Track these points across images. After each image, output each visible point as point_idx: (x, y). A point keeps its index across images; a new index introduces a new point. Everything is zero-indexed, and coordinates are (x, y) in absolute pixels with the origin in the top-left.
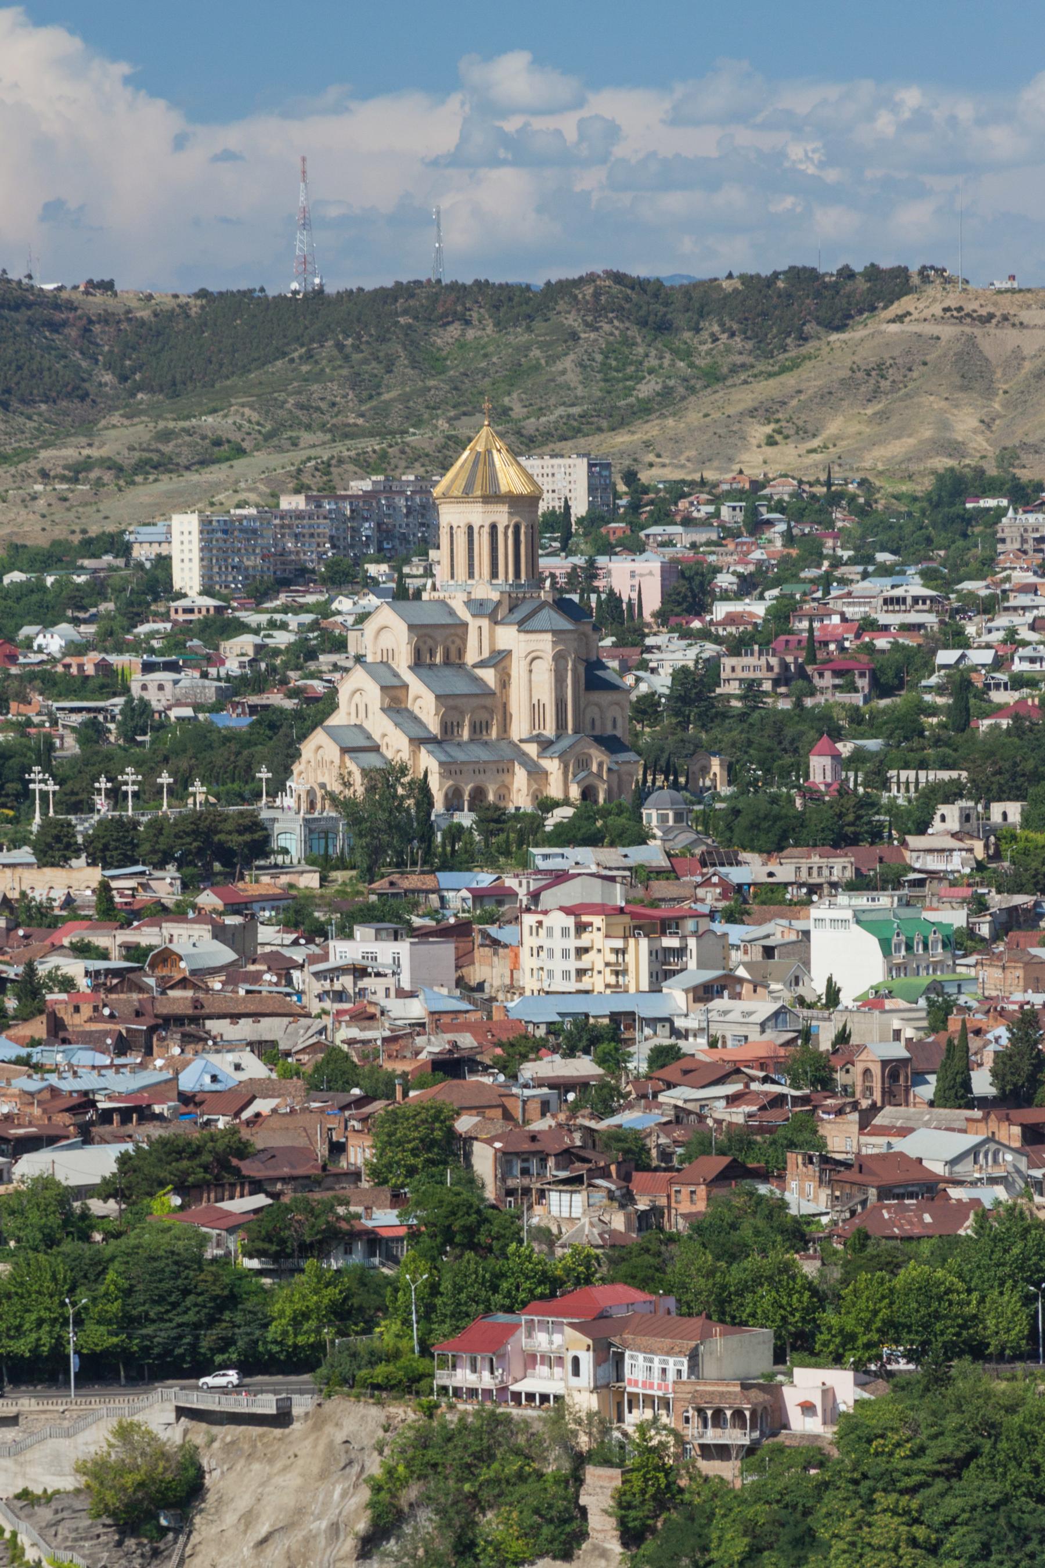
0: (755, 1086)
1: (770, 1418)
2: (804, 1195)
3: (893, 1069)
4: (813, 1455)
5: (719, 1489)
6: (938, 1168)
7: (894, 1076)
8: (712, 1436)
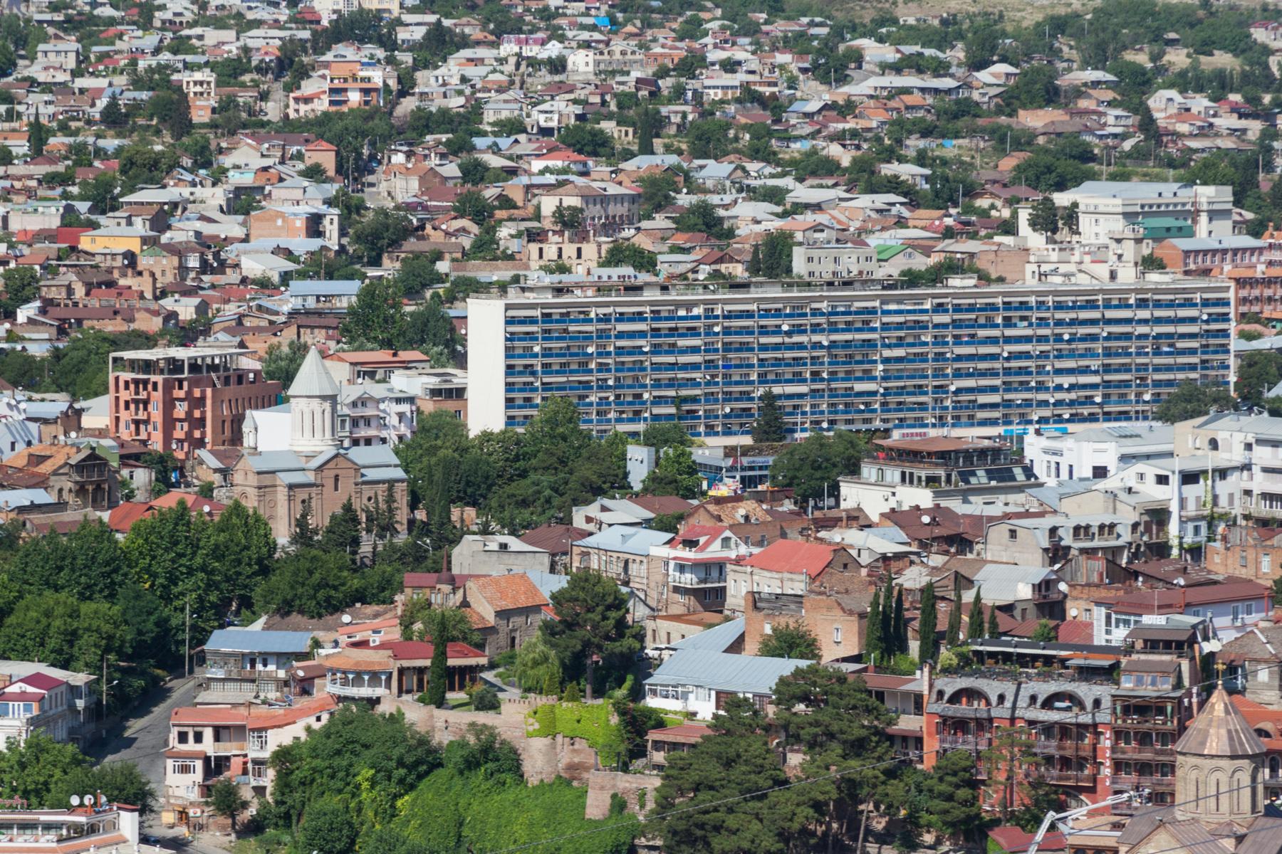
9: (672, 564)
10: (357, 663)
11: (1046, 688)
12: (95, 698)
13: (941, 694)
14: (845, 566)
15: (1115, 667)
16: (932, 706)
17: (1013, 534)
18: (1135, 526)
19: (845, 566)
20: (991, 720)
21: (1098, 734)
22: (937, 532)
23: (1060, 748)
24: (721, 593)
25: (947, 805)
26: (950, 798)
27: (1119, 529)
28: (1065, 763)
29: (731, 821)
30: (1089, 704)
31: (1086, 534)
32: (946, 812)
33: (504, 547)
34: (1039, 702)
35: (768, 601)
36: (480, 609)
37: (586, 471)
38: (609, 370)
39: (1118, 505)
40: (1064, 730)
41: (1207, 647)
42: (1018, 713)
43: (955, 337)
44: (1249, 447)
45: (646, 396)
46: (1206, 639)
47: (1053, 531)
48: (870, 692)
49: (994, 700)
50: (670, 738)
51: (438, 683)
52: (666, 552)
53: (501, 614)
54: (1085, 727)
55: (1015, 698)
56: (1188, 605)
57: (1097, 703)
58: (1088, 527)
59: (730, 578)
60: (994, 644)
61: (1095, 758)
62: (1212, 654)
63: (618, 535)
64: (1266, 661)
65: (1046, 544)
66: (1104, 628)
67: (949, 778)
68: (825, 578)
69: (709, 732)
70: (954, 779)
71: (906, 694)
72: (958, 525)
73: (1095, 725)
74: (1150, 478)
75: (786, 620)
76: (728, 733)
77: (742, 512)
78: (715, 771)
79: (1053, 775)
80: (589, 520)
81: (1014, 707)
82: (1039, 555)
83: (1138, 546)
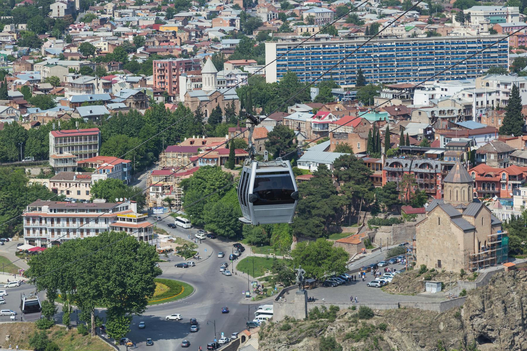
9: (313, 124)
11: (421, 162)
12: (131, 168)
13: (387, 164)
14: (365, 124)
15: (442, 154)
16: (385, 168)
17: (420, 113)
18: (460, 111)
19: (365, 124)
20: (403, 172)
22: (399, 113)
23: (425, 181)
25: (387, 200)
26: (388, 197)
27: (454, 111)
28: (426, 185)
29: (318, 205)
30: (434, 167)
31: (444, 113)
32: (387, 202)
35: (337, 135)
37: (295, 95)
38: (309, 65)
39: (456, 104)
41: (472, 148)
43: (397, 49)
44: (498, 85)
45: (321, 73)
46: (473, 145)
47: (432, 112)
48: (365, 164)
49: (404, 165)
50: (303, 179)
52: (312, 120)
54: (433, 174)
55: (409, 164)
56: (469, 135)
57: (437, 166)
58: (444, 111)
60: (411, 148)
61: (436, 184)
62: (475, 151)
64: (493, 153)
65: (430, 116)
66: (443, 142)
67: (388, 191)
68: (358, 128)
69: (312, 177)
70: (390, 191)
71: (377, 164)
72: (407, 111)
73: (436, 173)
74: (466, 96)
75: (343, 142)
76: (318, 177)
77: (337, 107)
78: (313, 188)
79: (422, 190)
80: (292, 110)
81: (410, 168)
83: (461, 117)
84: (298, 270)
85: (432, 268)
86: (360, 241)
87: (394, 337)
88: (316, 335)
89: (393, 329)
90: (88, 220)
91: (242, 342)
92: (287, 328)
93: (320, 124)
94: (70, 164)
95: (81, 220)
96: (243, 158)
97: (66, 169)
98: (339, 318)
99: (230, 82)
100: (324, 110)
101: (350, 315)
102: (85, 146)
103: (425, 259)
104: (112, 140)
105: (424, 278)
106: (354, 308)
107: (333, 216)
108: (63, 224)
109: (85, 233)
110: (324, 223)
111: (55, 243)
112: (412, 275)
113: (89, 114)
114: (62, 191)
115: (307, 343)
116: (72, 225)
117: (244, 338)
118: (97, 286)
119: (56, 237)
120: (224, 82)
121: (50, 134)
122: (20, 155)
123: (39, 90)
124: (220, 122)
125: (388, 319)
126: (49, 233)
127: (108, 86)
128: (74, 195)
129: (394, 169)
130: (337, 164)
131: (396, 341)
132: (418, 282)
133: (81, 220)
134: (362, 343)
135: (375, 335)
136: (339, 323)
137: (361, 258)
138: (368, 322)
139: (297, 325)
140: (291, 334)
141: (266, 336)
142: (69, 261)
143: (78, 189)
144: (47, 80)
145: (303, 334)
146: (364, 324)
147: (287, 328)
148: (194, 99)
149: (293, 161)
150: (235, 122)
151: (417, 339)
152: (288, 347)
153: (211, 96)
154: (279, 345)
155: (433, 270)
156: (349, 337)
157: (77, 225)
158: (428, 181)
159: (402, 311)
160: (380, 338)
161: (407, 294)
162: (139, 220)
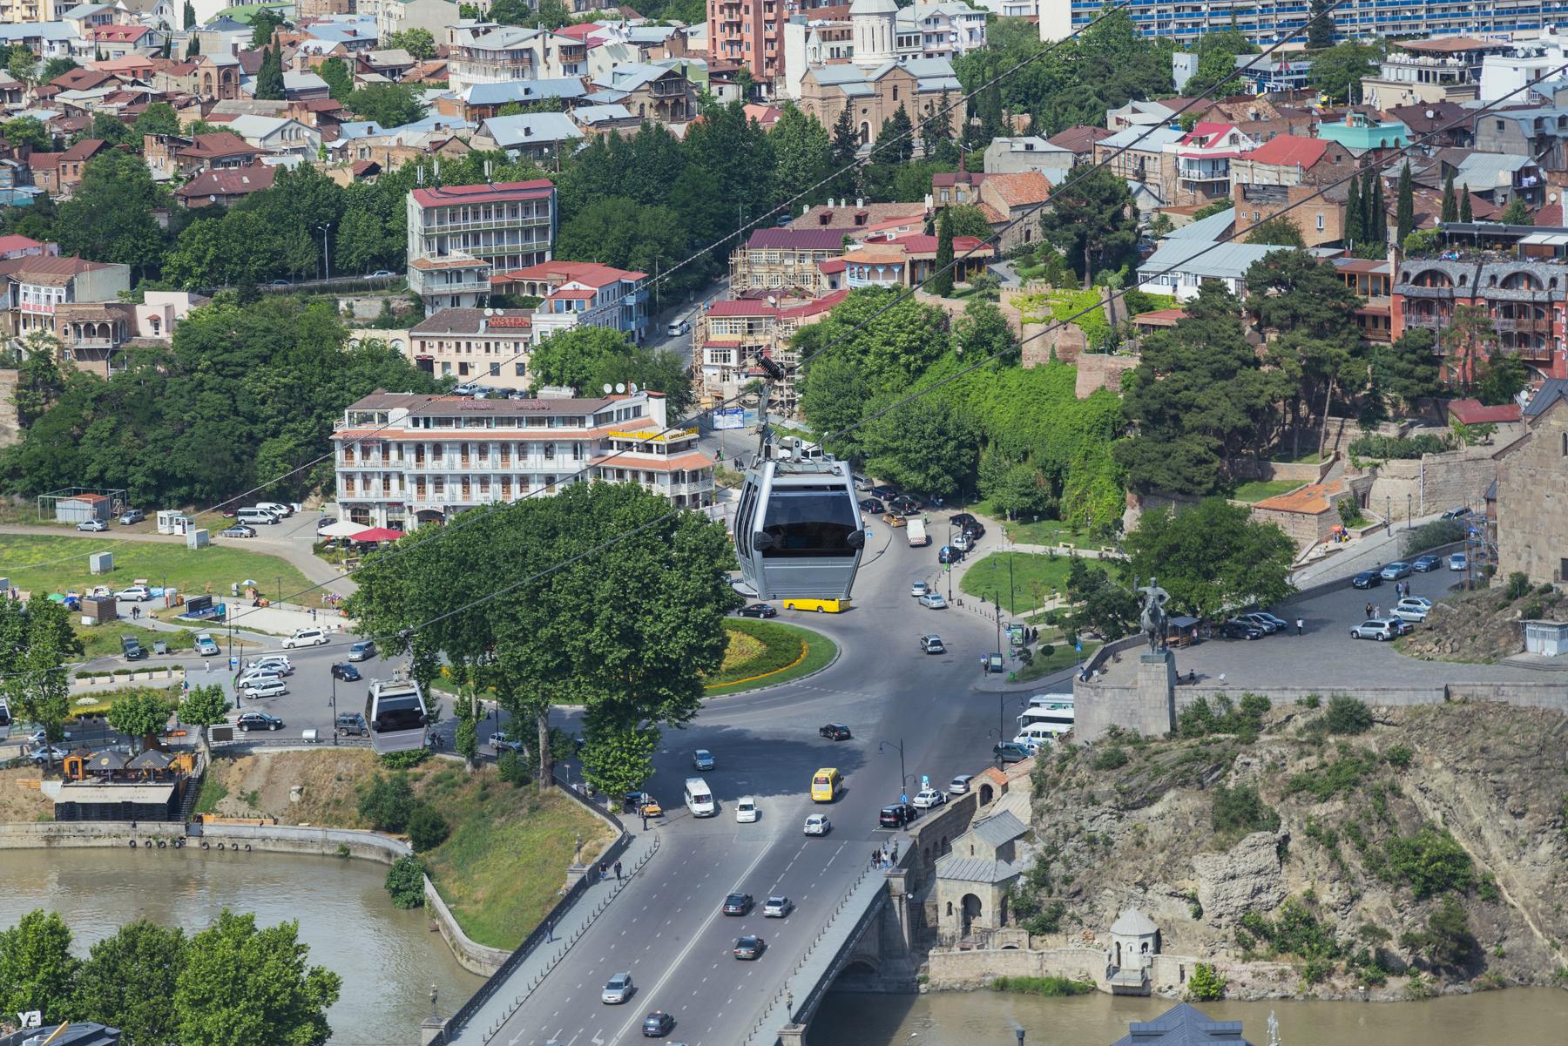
0: (126, 88)
1: (125, 328)
2: (160, 166)
3: (227, 73)
4: (157, 354)
5: (88, 382)
6: (255, 143)
7: (227, 77)
8: (84, 343)
9: (1182, 160)
10: (873, 257)
12: (647, 295)
13: (1406, 275)
14: (1339, 158)
16: (1398, 287)
17: (1501, 125)
20: (1453, 299)
21: (1554, 312)
23: (1519, 325)
24: (1225, 185)
25: (1407, 382)
26: (1408, 375)
28: (1523, 339)
29: (1202, 399)
30: (1546, 283)
32: (1406, 388)
33: (1030, 147)
34: (1499, 281)
35: (1256, 191)
36: (996, 205)
37: (1130, 76)
40: (1523, 307)
42: (1479, 292)
47: (1539, 122)
48: (1341, 277)
49: (1456, 280)
51: (946, 273)
52: (1181, 149)
53: (1013, 209)
54: (1542, 304)
57: (1554, 281)
59: (1233, 171)
60: (1476, 230)
61: (1551, 333)
63: (1145, 138)
65: (1532, 135)
67: (1408, 356)
71: (1376, 277)
73: (1551, 303)
77: (1252, 110)
78: (1185, 350)
79: (1511, 352)
80: (1119, 121)
81: (1475, 288)
82: (1524, 145)
84: (1148, 590)
85: (1543, 582)
86: (1328, 505)
87: (1433, 786)
88: (1200, 782)
89: (1431, 762)
90: (523, 448)
91: (983, 803)
92: (1115, 762)
93: (1203, 160)
94: (468, 285)
95: (504, 448)
96: (979, 263)
97: (456, 299)
98: (1270, 732)
99: (934, 38)
100: (1214, 118)
101: (1301, 721)
102: (513, 232)
103: (1524, 556)
104: (589, 218)
105: (1519, 613)
106: (1314, 703)
107: (1245, 432)
108: (451, 462)
109: (515, 487)
110: (1219, 452)
111: (426, 516)
112: (1484, 604)
113: (521, 138)
114: (446, 365)
115: (1175, 804)
116: (476, 465)
117: (987, 791)
118: (555, 642)
119: (433, 500)
120: (917, 38)
121: (410, 197)
122: (321, 260)
123: (374, 70)
124: (907, 157)
125: (1415, 734)
126: (411, 488)
127: (575, 55)
128: (480, 375)
129: (1427, 290)
130: (1256, 278)
131: (1437, 799)
132: (1504, 625)
133: (504, 448)
134: (1340, 805)
135: (1377, 782)
136: (1268, 746)
137: (1330, 553)
138: (1356, 742)
139: (1145, 754)
140: (1128, 780)
141: (1055, 783)
142: (472, 568)
143: (492, 357)
144: (397, 41)
145: (1164, 778)
146: (1343, 749)
147: (1115, 762)
148: (830, 91)
149: (1125, 269)
150: (951, 156)
151: (1501, 793)
152: (1120, 818)
153: (879, 80)
154: (1092, 811)
155: (1548, 589)
156: (1298, 786)
157: (491, 464)
158: (1527, 325)
159: (1457, 709)
160: (1392, 789)
161: (1471, 661)
162: (673, 448)
